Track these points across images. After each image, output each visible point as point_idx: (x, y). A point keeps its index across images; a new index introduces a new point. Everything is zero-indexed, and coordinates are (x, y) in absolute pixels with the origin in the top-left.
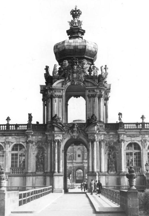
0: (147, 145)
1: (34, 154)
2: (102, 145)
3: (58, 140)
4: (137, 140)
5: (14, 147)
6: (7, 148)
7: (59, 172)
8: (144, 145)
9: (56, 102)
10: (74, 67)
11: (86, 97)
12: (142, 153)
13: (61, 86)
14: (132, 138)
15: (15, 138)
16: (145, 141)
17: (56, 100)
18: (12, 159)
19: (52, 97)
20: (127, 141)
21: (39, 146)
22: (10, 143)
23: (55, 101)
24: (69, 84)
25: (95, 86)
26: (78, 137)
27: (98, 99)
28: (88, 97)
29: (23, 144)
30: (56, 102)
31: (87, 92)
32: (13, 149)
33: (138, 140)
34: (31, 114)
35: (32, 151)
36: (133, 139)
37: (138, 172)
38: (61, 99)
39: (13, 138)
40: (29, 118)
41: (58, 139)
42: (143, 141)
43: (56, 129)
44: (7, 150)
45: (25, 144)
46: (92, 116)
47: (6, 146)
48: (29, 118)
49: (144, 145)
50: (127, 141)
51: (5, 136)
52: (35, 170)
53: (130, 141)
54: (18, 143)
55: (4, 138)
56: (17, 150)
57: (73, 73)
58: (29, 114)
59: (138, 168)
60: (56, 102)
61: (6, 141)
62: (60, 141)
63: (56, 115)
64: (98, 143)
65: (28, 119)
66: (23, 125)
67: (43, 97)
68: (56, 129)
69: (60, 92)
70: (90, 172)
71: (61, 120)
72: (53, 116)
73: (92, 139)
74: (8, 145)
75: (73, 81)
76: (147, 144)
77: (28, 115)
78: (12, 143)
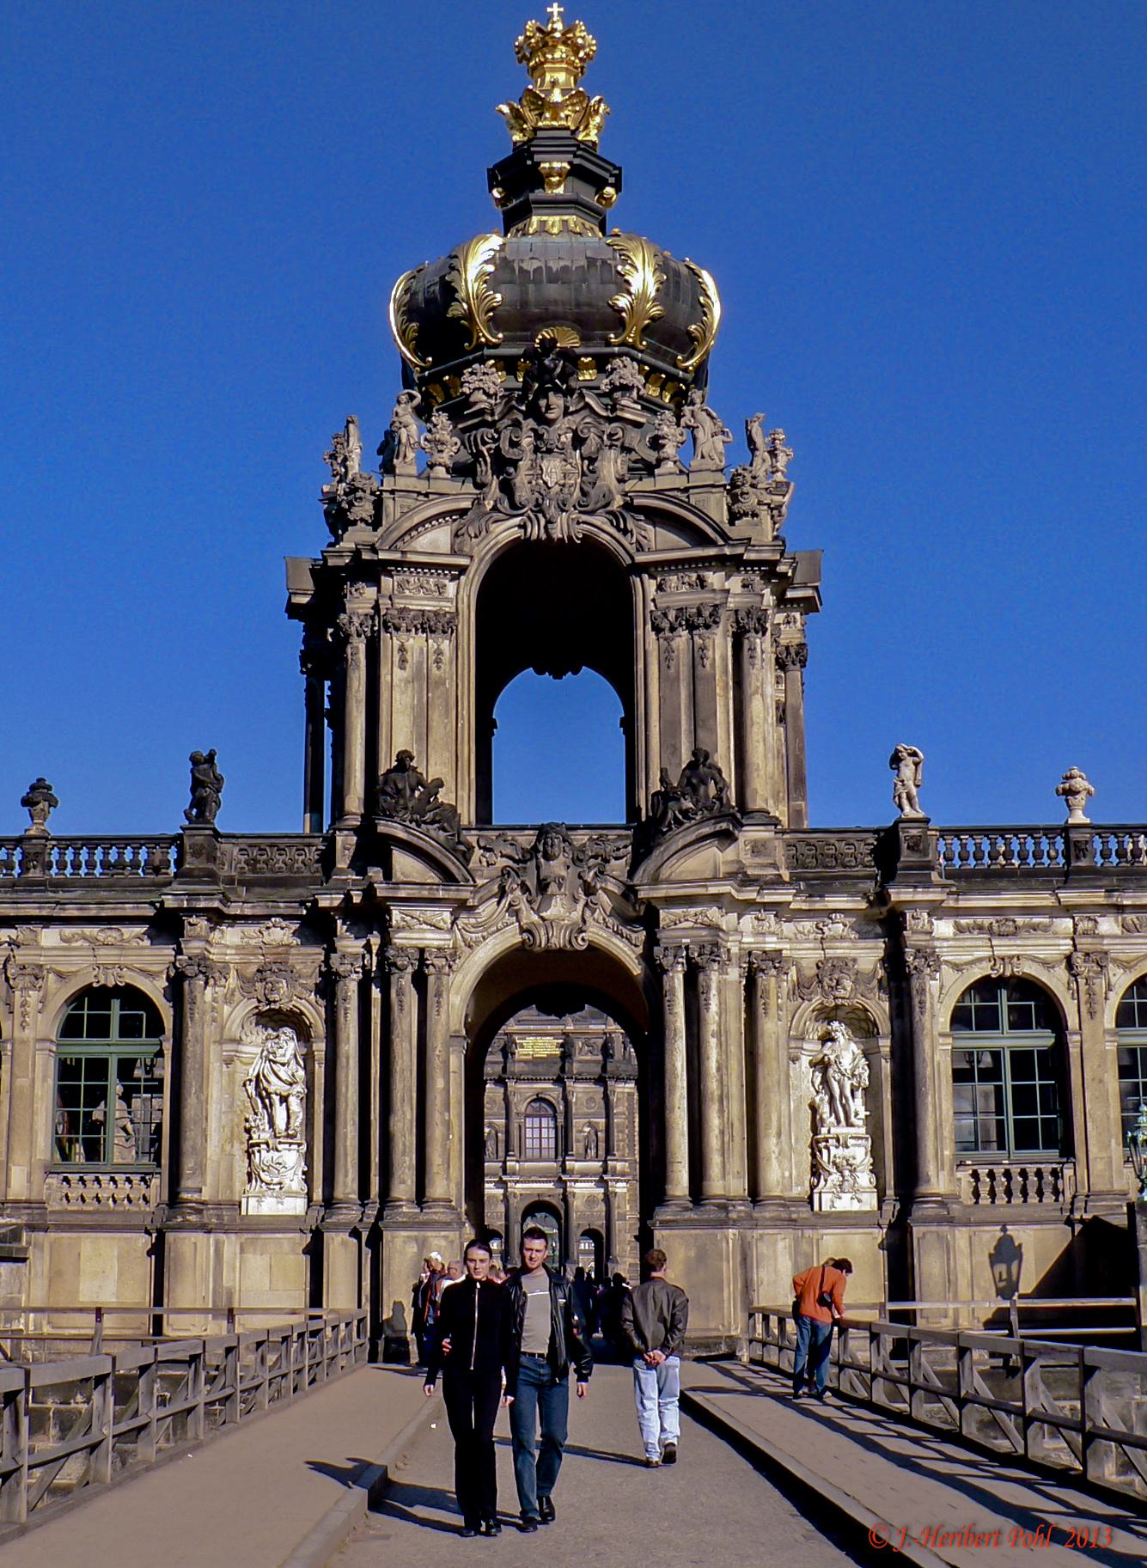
0: (1111, 994)
2: (766, 992)
3: (422, 951)
4: (1034, 959)
6: (24, 1015)
7: (421, 1197)
8: (1090, 993)
9: (403, 661)
10: (548, 407)
11: (640, 632)
12: (1074, 1051)
13: (447, 549)
14: (995, 942)
16: (1100, 960)
17: (402, 649)
18: (66, 1096)
19: (381, 623)
20: (957, 967)
21: (269, 1003)
22: (51, 976)
23: (396, 658)
24: (505, 531)
25: (706, 541)
26: (581, 931)
27: (730, 641)
28: (657, 629)
30: (403, 661)
31: (646, 588)
32: (71, 1028)
33: (1042, 954)
34: (211, 756)
35: (220, 1042)
36: (1004, 948)
37: (1049, 1198)
38: (446, 645)
40: (193, 790)
41: (421, 944)
42: (1078, 959)
43: (403, 863)
46: (692, 766)
48: (197, 784)
49: (1090, 993)
50: (957, 967)
53: (980, 960)
54: (110, 984)
57: (542, 448)
59: (1046, 1168)
60: (408, 666)
62: (437, 962)
63: (404, 758)
64: (734, 974)
65: (190, 797)
67: (305, 641)
68: (403, 863)
69: (441, 588)
70: (679, 1197)
71: (445, 796)
72: (383, 767)
73: (687, 948)
75: (539, 508)
76: (1109, 988)
77: (191, 766)
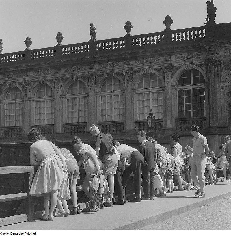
1: (223, 88)
5: (182, 76)
6: (168, 80)
15: (182, 57)
18: (180, 100)
29: (199, 69)
32: (180, 82)
39: (177, 58)
44: (167, 83)
45: (204, 68)
47: (165, 76)
51: (162, 55)
52: (227, 122)
54: (189, 69)
55: (162, 59)
56: (188, 82)
58: (208, 3)
61: (165, 65)
66: (198, 29)
74: (170, 74)
78: (177, 68)
